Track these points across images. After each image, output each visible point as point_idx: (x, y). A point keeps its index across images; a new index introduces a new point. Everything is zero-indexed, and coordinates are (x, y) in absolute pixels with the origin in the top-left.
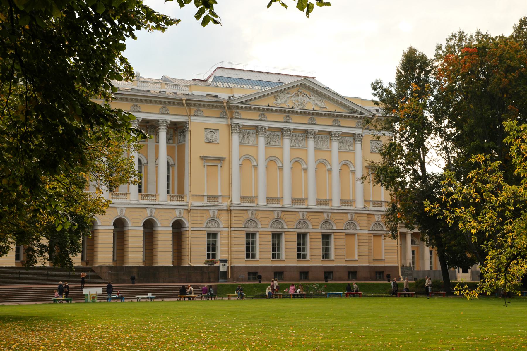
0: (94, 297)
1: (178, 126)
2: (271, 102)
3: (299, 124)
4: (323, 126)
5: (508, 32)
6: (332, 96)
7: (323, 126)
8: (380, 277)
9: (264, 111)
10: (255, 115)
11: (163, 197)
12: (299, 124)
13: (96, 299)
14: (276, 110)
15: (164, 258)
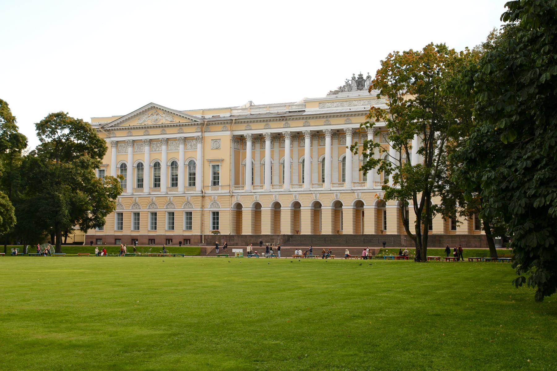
0: (238, 255)
1: (300, 135)
2: (135, 123)
3: (155, 135)
4: (172, 134)
5: (498, 26)
6: (130, 116)
7: (172, 134)
8: (152, 243)
9: (130, 129)
10: (125, 133)
11: (267, 186)
12: (155, 135)
13: (240, 256)
14: (140, 128)
15: (226, 229)
